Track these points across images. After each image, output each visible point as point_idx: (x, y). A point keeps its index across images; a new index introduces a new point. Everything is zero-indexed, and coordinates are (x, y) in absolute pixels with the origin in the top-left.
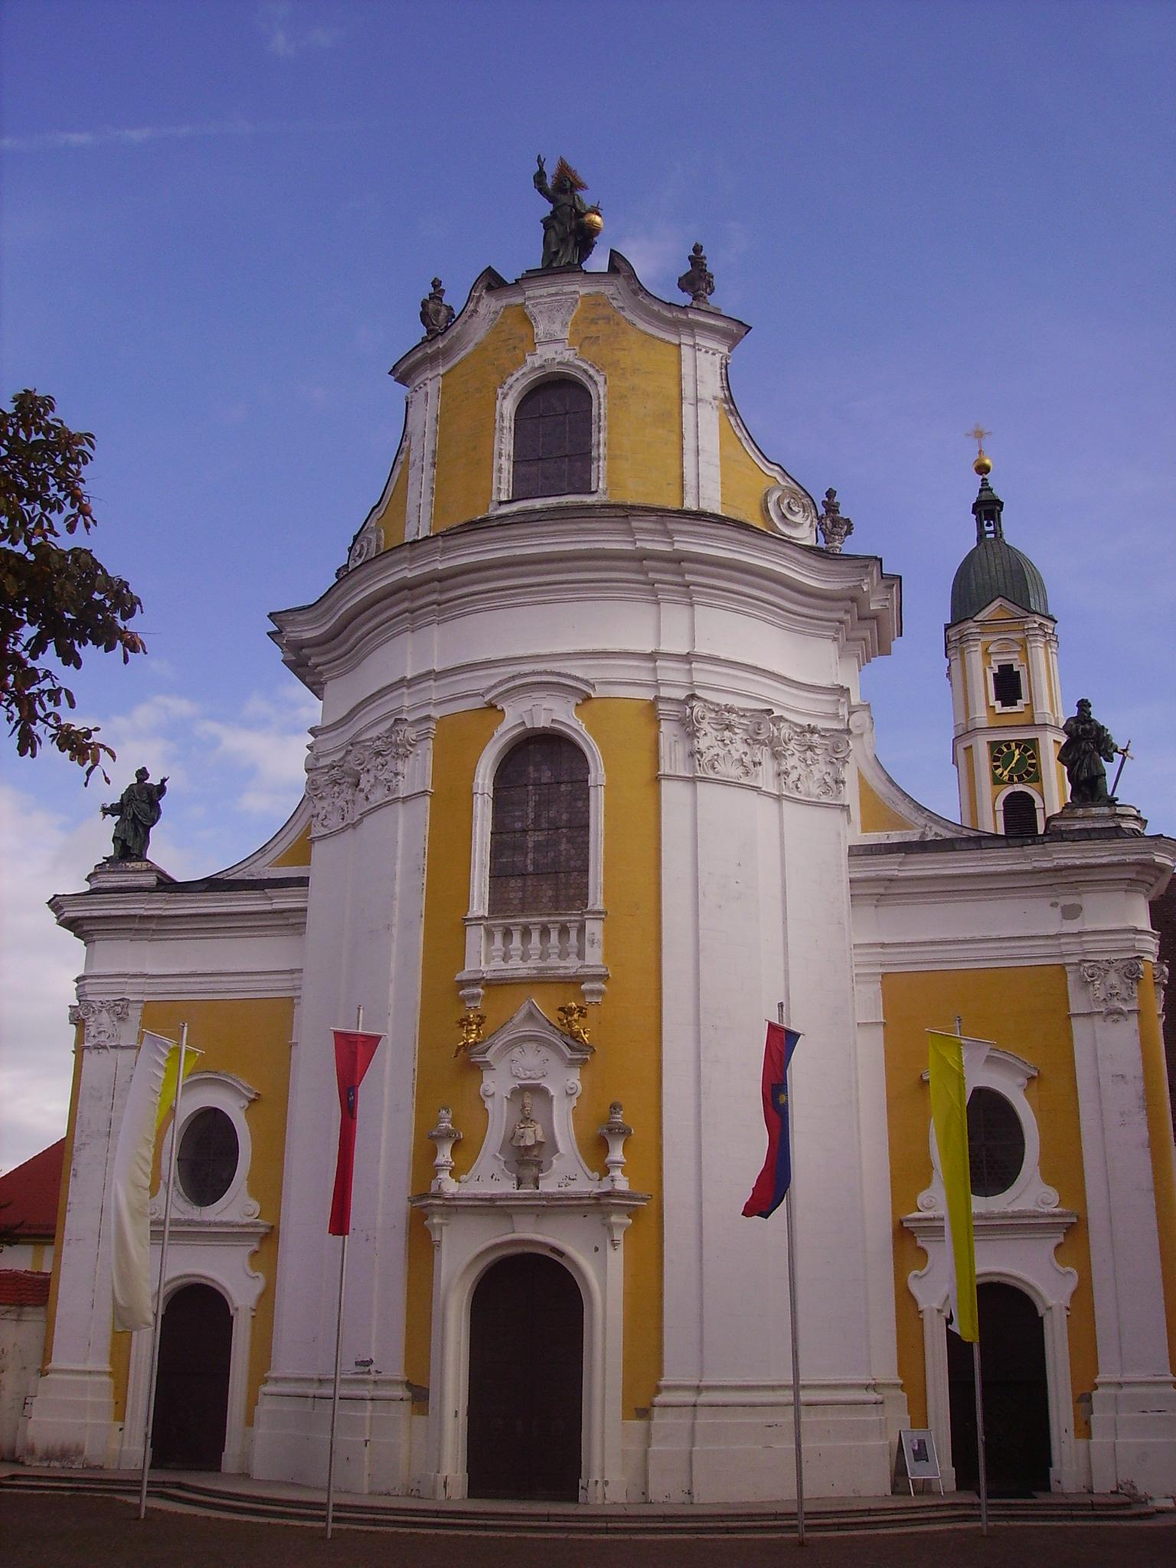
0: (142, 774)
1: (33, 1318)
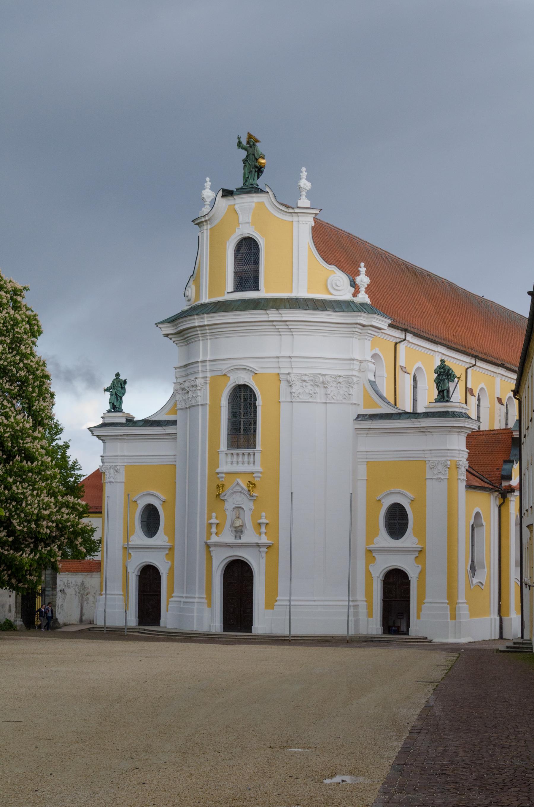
0: (118, 375)
1: (96, 575)
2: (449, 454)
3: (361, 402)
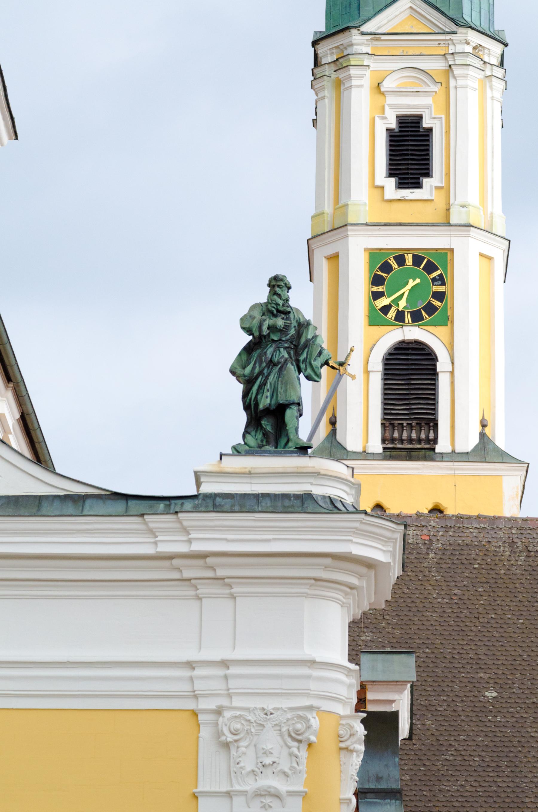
2: (314, 686)
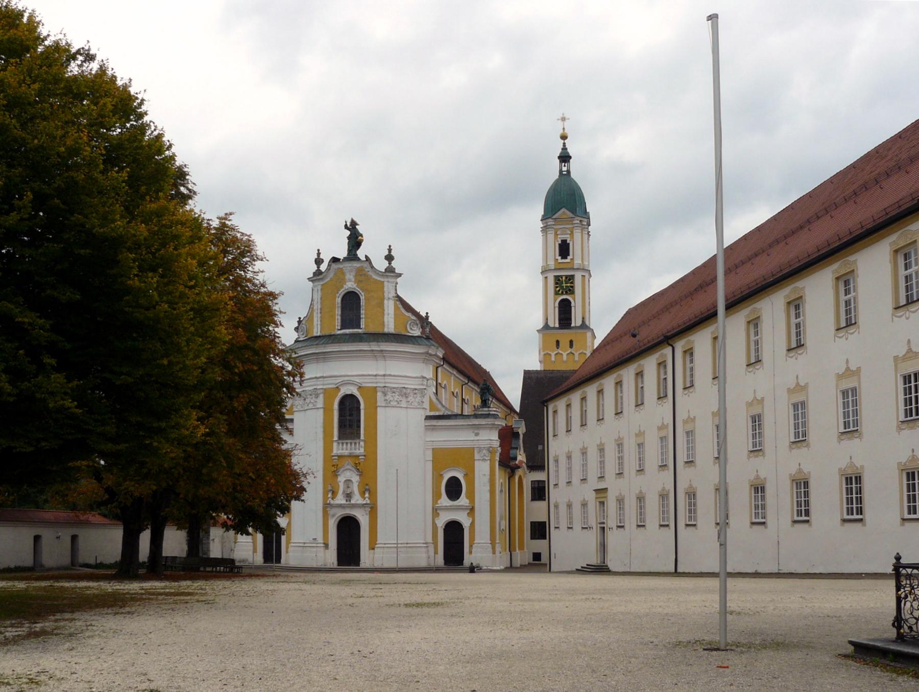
3: (428, 407)
